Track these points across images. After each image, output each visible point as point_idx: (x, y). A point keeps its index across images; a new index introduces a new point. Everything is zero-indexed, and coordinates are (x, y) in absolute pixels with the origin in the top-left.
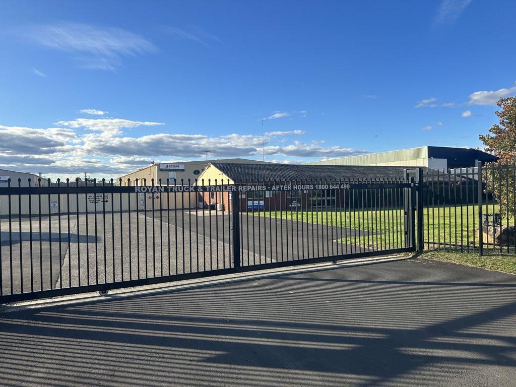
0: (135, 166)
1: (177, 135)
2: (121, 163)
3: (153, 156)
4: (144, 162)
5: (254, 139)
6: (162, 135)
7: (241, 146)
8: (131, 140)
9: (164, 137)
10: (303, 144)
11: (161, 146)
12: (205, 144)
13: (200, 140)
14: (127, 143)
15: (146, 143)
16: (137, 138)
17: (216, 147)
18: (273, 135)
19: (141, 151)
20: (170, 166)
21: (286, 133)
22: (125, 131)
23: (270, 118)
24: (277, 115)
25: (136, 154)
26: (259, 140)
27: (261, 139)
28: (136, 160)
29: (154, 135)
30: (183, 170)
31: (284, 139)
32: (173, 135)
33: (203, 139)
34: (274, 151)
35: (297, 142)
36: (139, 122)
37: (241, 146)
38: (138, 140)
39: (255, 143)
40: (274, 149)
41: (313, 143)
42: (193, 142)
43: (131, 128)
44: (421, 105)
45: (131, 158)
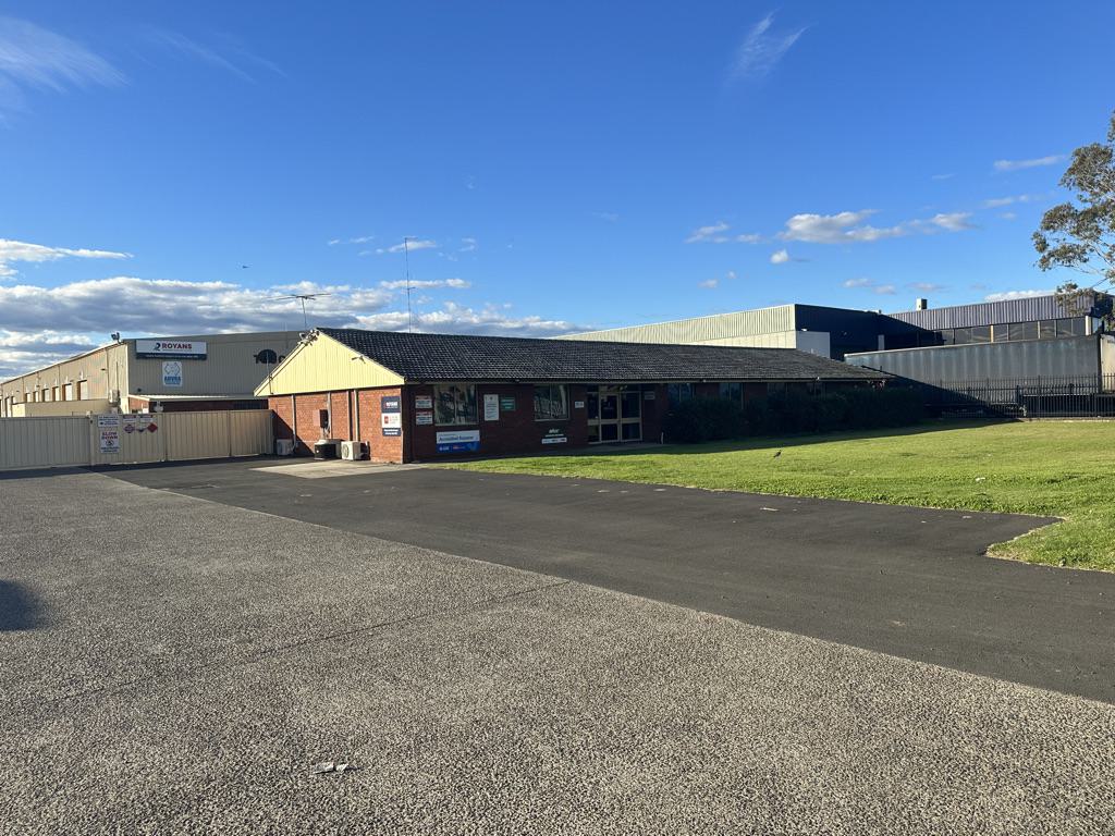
0: (44, 355)
1: (160, 283)
2: (7, 348)
3: (93, 333)
4: (70, 347)
5: (353, 296)
6: (120, 281)
7: (323, 310)
8: (35, 293)
9: (125, 284)
10: (466, 309)
11: (117, 307)
12: (230, 304)
13: (220, 295)
14: (24, 300)
15: (75, 299)
16: (50, 289)
17: (257, 313)
18: (400, 288)
19: (62, 319)
20: (164, 345)
21: (430, 283)
22: (24, 271)
23: (393, 249)
24: (411, 245)
25: (50, 327)
26: (367, 298)
27: (373, 296)
28: (48, 342)
29: (98, 280)
30: (202, 357)
31: (423, 297)
32: (148, 281)
33: (227, 293)
34: (399, 323)
35: (452, 306)
36: (61, 250)
37: (323, 310)
38: (56, 292)
39: (356, 304)
40: (398, 319)
41: (487, 309)
42: (201, 298)
43: (39, 264)
44: (699, 237)
45: (34, 338)
